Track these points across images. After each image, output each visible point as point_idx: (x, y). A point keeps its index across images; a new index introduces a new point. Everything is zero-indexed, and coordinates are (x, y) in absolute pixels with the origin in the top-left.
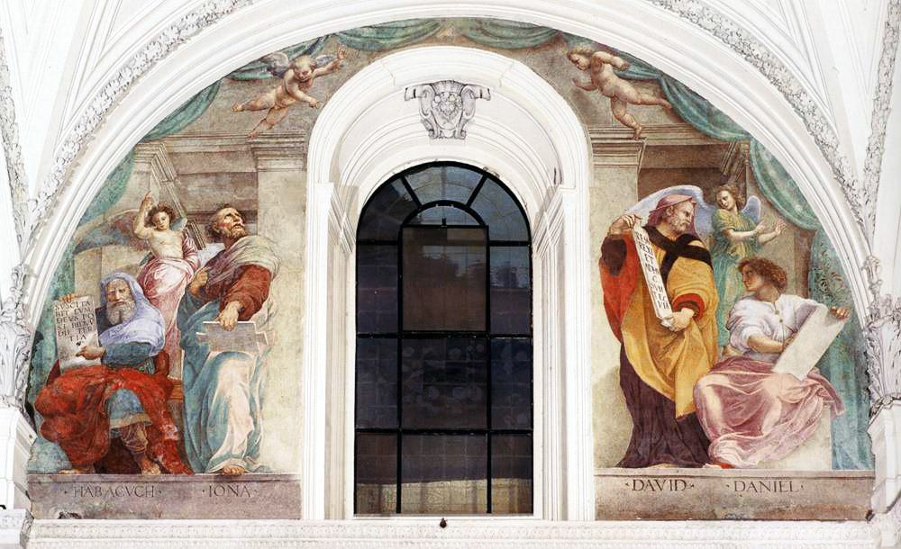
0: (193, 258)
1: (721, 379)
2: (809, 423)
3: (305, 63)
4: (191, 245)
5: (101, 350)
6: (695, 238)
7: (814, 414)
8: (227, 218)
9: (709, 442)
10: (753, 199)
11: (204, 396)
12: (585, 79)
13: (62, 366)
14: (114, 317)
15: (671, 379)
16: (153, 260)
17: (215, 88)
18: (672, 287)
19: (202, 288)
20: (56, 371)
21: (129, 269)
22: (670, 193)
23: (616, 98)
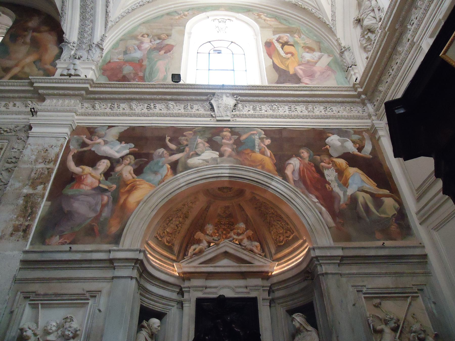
0: (153, 43)
1: (301, 67)
2: (328, 76)
3: (186, 13)
4: (152, 40)
5: (123, 58)
6: (289, 42)
7: (329, 74)
8: (163, 36)
9: (301, 79)
10: (303, 36)
11: (152, 68)
12: (257, 17)
13: (111, 61)
14: (128, 52)
15: (288, 67)
16: (142, 43)
17: (162, 16)
18: (284, 50)
19: (154, 48)
20: (110, 62)
21: (135, 44)
22: (282, 35)
23: (265, 20)
